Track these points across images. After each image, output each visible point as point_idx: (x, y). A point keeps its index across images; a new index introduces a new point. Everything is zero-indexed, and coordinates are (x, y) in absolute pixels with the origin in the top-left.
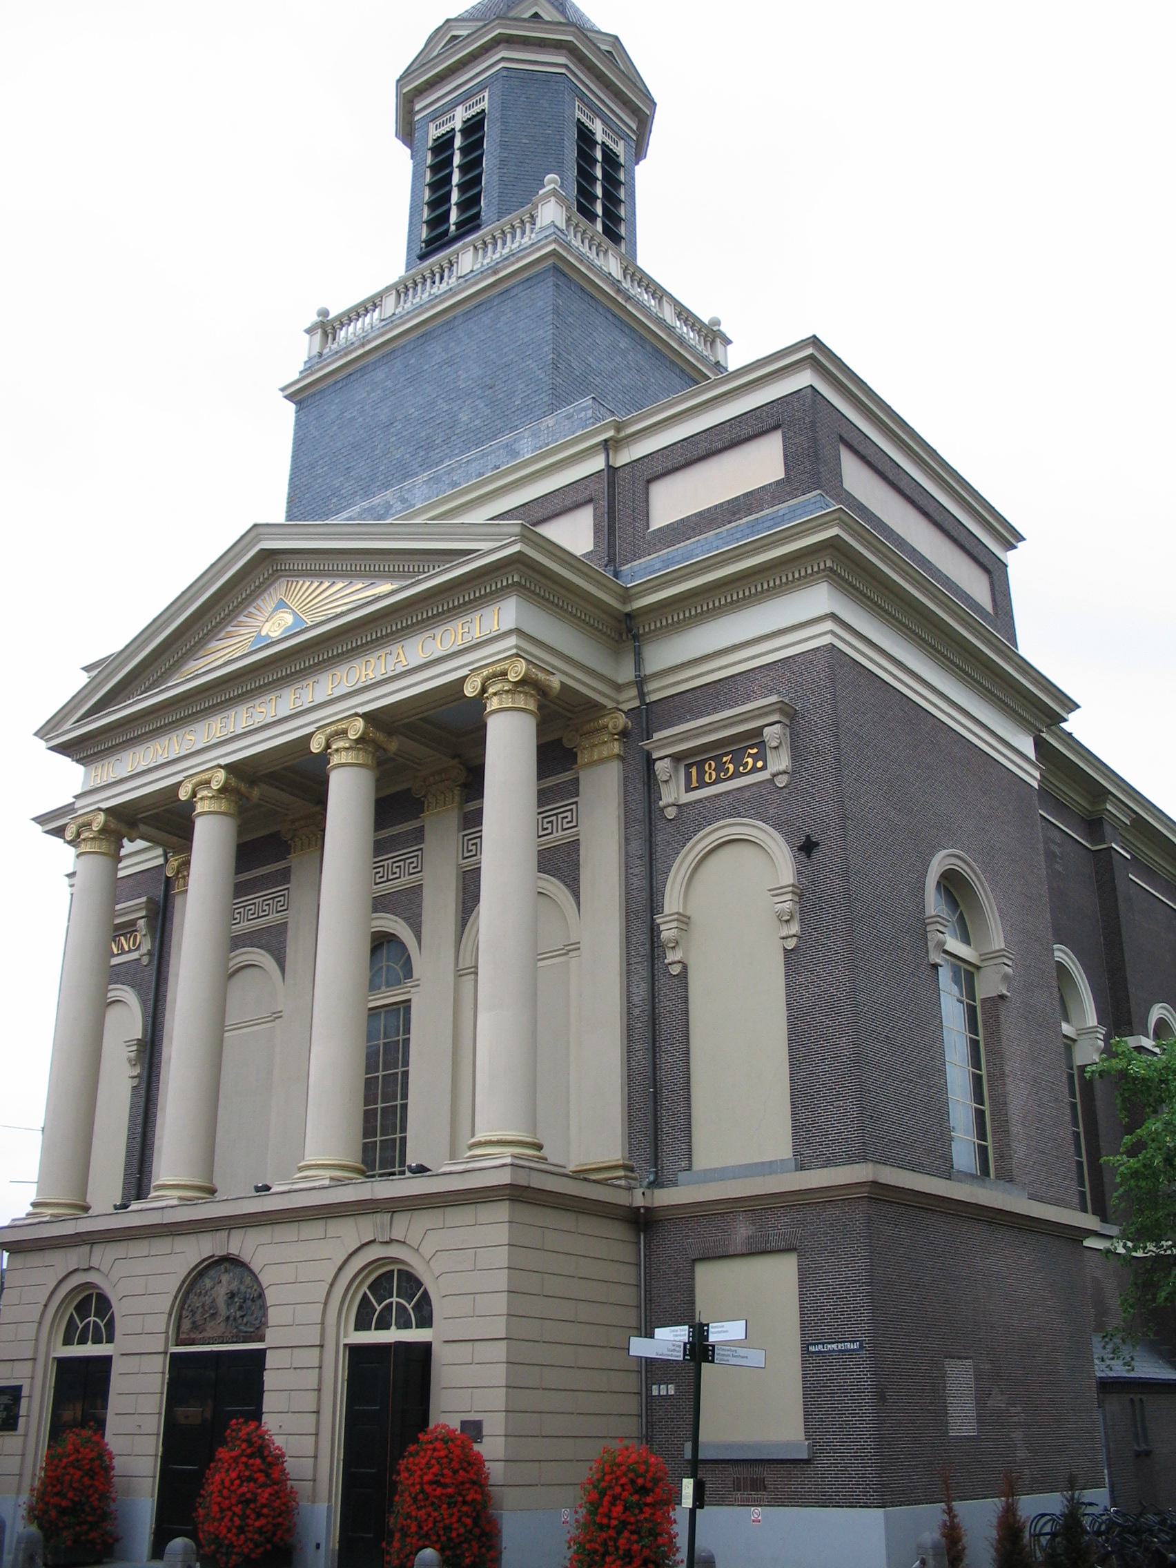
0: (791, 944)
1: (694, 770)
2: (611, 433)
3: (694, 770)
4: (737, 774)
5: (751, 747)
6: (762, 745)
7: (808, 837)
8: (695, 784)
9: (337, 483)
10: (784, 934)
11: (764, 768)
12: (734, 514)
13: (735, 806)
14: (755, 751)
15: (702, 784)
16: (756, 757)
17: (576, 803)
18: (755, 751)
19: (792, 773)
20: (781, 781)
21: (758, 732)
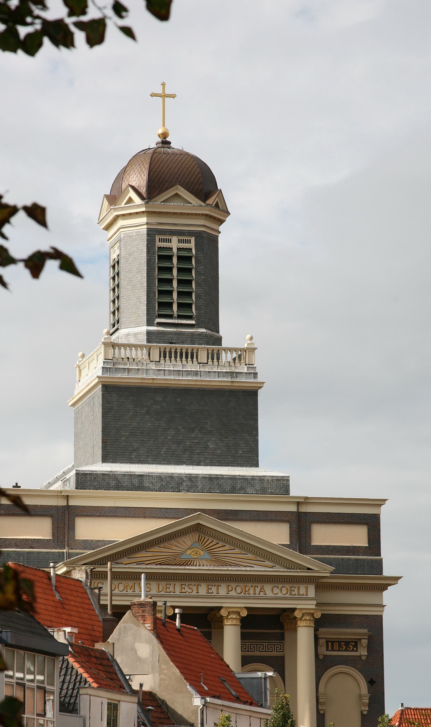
0: (365, 713)
1: (330, 644)
2: (303, 500)
3: (330, 644)
4: (346, 650)
5: (353, 642)
6: (356, 643)
7: (372, 679)
8: (330, 649)
9: (136, 445)
10: (363, 709)
11: (357, 651)
12: (348, 552)
13: (345, 661)
14: (353, 644)
15: (333, 650)
16: (354, 647)
17: (283, 643)
18: (353, 644)
19: (367, 656)
20: (364, 658)
21: (360, 639)
